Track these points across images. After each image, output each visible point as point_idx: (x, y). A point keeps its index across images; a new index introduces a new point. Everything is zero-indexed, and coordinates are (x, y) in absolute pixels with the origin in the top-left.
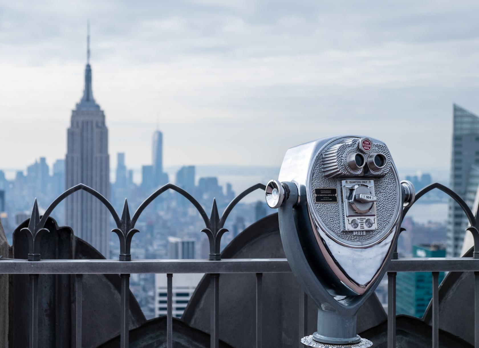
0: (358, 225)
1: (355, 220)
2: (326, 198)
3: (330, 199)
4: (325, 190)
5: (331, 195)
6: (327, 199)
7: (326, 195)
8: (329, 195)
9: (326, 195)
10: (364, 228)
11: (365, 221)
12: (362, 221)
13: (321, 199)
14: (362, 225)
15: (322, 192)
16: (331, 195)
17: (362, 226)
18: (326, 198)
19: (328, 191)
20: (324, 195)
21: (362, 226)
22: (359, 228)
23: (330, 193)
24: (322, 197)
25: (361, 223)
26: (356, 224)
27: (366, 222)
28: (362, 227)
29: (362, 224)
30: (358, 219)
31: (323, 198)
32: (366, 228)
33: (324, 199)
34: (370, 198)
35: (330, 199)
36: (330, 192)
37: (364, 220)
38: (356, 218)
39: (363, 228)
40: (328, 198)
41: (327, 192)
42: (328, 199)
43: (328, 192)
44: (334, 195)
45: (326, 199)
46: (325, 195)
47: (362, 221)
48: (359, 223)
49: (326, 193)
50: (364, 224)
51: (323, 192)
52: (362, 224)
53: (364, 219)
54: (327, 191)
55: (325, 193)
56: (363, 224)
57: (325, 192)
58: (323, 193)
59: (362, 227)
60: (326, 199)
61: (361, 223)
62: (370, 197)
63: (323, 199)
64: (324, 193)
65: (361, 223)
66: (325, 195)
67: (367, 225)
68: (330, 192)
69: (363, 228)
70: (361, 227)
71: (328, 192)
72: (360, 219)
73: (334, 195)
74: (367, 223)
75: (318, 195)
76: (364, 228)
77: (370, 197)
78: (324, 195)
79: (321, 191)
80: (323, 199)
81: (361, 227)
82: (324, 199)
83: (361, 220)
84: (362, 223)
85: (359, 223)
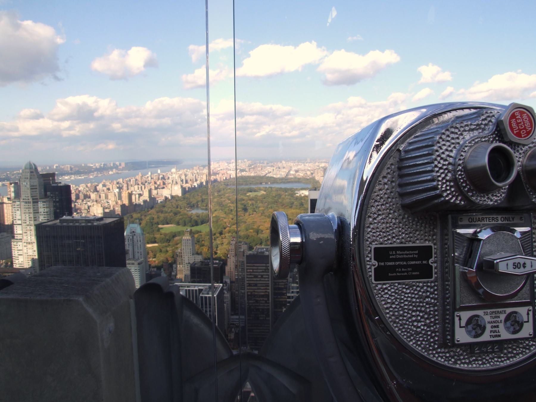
0: (483, 329)
1: (478, 316)
2: (403, 270)
6: (406, 274)
7: (405, 263)
8: (413, 263)
9: (405, 263)
10: (500, 336)
11: (503, 317)
13: (390, 275)
14: (494, 329)
17: (495, 331)
18: (403, 270)
19: (411, 252)
20: (397, 263)
21: (495, 331)
22: (486, 337)
23: (415, 256)
24: (393, 269)
25: (492, 324)
26: (480, 326)
27: (507, 319)
28: (495, 334)
29: (495, 327)
30: (486, 314)
31: (396, 272)
32: (505, 335)
33: (398, 274)
34: (524, 267)
38: (480, 312)
39: (496, 336)
40: (409, 269)
42: (407, 272)
43: (411, 254)
45: (404, 272)
46: (401, 263)
47: (496, 317)
48: (489, 322)
49: (405, 256)
50: (502, 326)
51: (396, 254)
52: (495, 327)
53: (501, 312)
54: (408, 253)
55: (402, 256)
56: (498, 327)
57: (403, 254)
58: (394, 257)
59: (495, 334)
60: (404, 272)
61: (494, 322)
62: (524, 264)
63: (395, 274)
64: (398, 256)
65: (494, 322)
66: (401, 263)
67: (507, 329)
69: (496, 336)
70: (492, 334)
71: (411, 254)
72: (493, 312)
74: (508, 324)
75: (382, 264)
76: (500, 336)
77: (524, 264)
78: (397, 263)
79: (391, 253)
80: (395, 274)
81: (492, 334)
82: (398, 274)
85: (489, 322)
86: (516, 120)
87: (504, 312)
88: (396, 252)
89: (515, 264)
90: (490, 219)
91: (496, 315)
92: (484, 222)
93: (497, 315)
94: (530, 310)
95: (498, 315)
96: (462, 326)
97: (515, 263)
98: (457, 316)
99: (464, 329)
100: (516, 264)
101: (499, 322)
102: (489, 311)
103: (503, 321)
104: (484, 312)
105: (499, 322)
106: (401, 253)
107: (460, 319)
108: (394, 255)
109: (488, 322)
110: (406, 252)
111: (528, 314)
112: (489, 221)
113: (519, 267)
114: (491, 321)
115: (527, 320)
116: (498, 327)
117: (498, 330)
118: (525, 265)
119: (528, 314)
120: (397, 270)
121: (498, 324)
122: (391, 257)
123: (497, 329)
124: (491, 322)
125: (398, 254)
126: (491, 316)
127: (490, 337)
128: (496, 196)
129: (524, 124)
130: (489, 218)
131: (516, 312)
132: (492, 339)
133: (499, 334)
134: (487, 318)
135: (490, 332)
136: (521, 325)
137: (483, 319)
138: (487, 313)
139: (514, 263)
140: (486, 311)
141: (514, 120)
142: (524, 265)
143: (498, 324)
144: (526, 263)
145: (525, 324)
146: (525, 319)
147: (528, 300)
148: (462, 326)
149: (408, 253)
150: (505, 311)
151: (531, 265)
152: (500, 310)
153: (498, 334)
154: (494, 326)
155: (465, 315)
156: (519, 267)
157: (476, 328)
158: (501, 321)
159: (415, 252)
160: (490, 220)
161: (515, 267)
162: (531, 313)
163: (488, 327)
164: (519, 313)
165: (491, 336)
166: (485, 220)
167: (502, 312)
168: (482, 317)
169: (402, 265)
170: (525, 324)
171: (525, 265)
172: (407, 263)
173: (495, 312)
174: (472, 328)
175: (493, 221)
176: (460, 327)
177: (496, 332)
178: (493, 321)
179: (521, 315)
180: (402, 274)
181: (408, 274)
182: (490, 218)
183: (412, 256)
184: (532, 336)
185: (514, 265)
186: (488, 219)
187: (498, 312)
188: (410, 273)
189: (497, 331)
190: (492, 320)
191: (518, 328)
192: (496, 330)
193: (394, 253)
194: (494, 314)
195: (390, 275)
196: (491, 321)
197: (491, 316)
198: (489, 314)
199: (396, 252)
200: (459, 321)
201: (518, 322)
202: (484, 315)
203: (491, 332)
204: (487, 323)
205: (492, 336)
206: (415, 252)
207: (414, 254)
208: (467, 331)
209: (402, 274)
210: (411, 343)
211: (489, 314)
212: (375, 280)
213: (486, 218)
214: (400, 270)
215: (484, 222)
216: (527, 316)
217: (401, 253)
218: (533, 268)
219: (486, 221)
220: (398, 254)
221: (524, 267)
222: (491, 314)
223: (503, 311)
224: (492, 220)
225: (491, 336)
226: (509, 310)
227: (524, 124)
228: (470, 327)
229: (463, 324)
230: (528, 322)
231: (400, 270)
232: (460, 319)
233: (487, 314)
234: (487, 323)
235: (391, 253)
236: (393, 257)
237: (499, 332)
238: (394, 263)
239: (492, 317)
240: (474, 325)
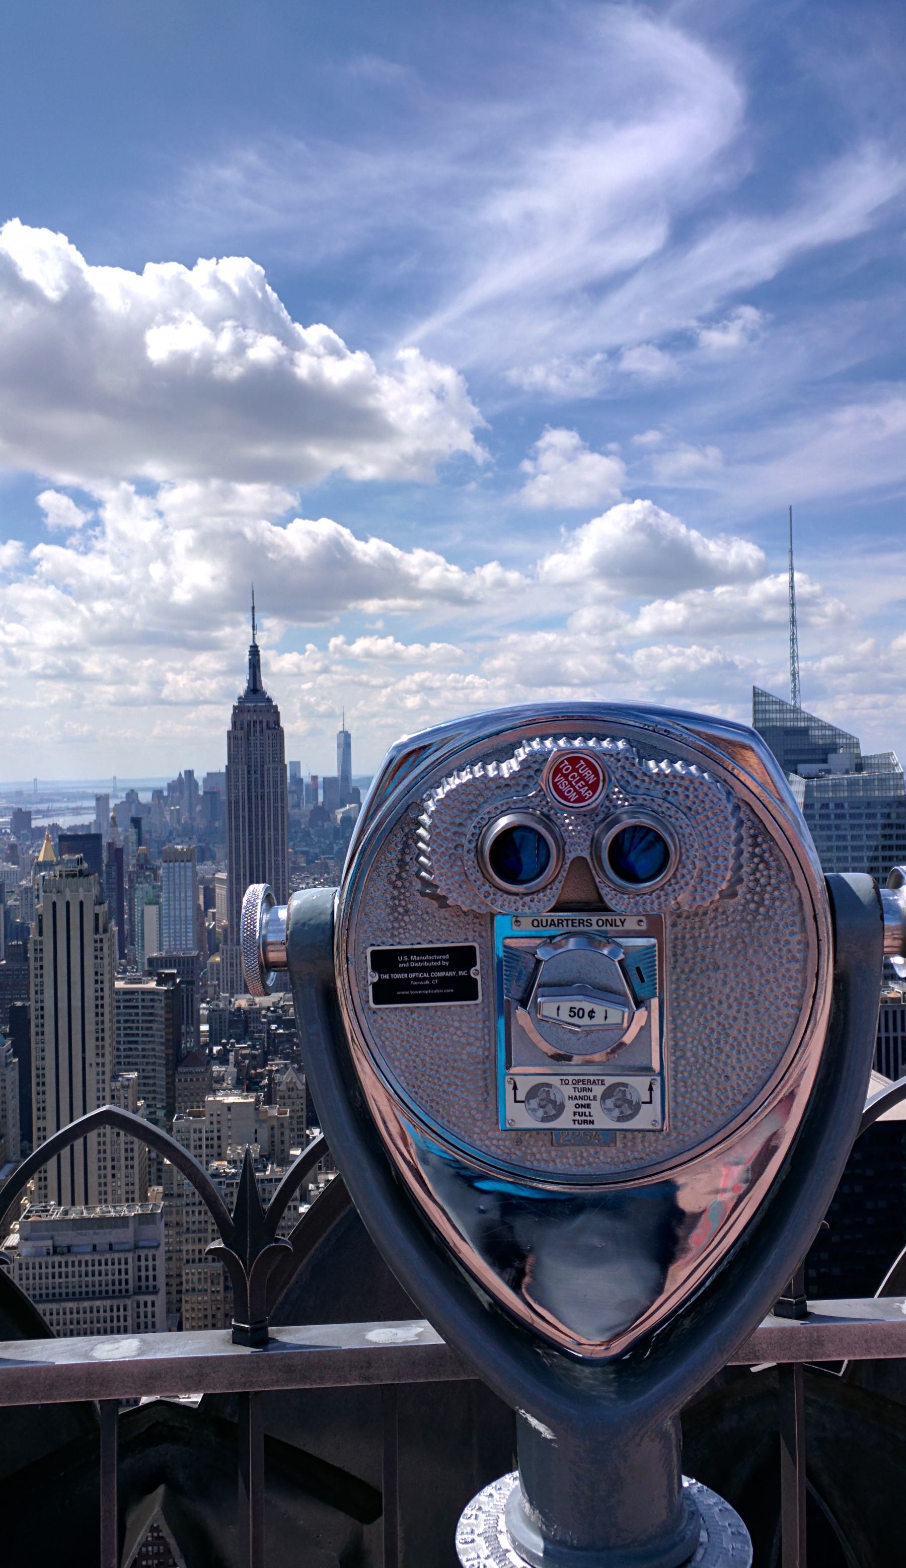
1: (549, 1085)
7: (426, 975)
8: (442, 974)
9: (426, 975)
10: (592, 1122)
11: (598, 1090)
12: (584, 1093)
13: (399, 993)
14: (580, 1110)
17: (584, 1114)
20: (413, 975)
21: (584, 1114)
22: (565, 1121)
23: (444, 963)
25: (576, 1102)
27: (605, 1096)
28: (583, 1118)
29: (583, 1106)
32: (603, 1120)
34: (591, 1017)
36: (445, 960)
37: (594, 1087)
39: (585, 1122)
41: (428, 961)
43: (437, 961)
46: (420, 975)
47: (584, 1090)
49: (426, 964)
50: (596, 1106)
51: (410, 961)
52: (583, 1106)
54: (430, 958)
55: (420, 964)
56: (588, 1106)
57: (422, 961)
58: (407, 965)
59: (583, 1118)
61: (582, 1098)
62: (592, 1011)
64: (413, 965)
65: (582, 1098)
66: (420, 975)
68: (445, 960)
69: (585, 1122)
70: (577, 1117)
71: (437, 961)
72: (578, 1081)
74: (610, 1103)
76: (592, 1122)
77: (592, 1011)
78: (413, 975)
79: (400, 959)
81: (577, 1117)
83: (580, 1086)
84: (580, 1102)
88: (409, 958)
93: (587, 1086)
95: (590, 1086)
96: (518, 1099)
100: (576, 1011)
101: (592, 1098)
103: (599, 1098)
105: (592, 1098)
106: (418, 958)
107: (515, 1088)
108: (405, 962)
111: (651, 1089)
113: (581, 1015)
119: (651, 1089)
121: (588, 1102)
122: (400, 965)
123: (587, 1110)
125: (414, 961)
131: (625, 1085)
132: (577, 1126)
133: (591, 1119)
136: (636, 1109)
142: (591, 1014)
143: (588, 1102)
145: (643, 1106)
148: (518, 1099)
149: (430, 958)
150: (602, 1081)
153: (588, 1118)
156: (581, 1015)
158: (595, 1098)
159: (444, 957)
161: (572, 1014)
163: (570, 1106)
164: (632, 1087)
165: (574, 1121)
168: (556, 1087)
176: (516, 1101)
179: (635, 1090)
187: (589, 1081)
190: (578, 1094)
193: (406, 958)
199: (409, 958)
200: (513, 1092)
203: (575, 1114)
206: (444, 957)
207: (441, 960)
220: (414, 961)
221: (591, 1017)
225: (574, 1121)
229: (521, 1096)
230: (650, 1102)
232: (515, 1088)
234: (567, 1098)
235: (400, 959)
236: (404, 965)
237: (590, 1115)
238: (406, 975)
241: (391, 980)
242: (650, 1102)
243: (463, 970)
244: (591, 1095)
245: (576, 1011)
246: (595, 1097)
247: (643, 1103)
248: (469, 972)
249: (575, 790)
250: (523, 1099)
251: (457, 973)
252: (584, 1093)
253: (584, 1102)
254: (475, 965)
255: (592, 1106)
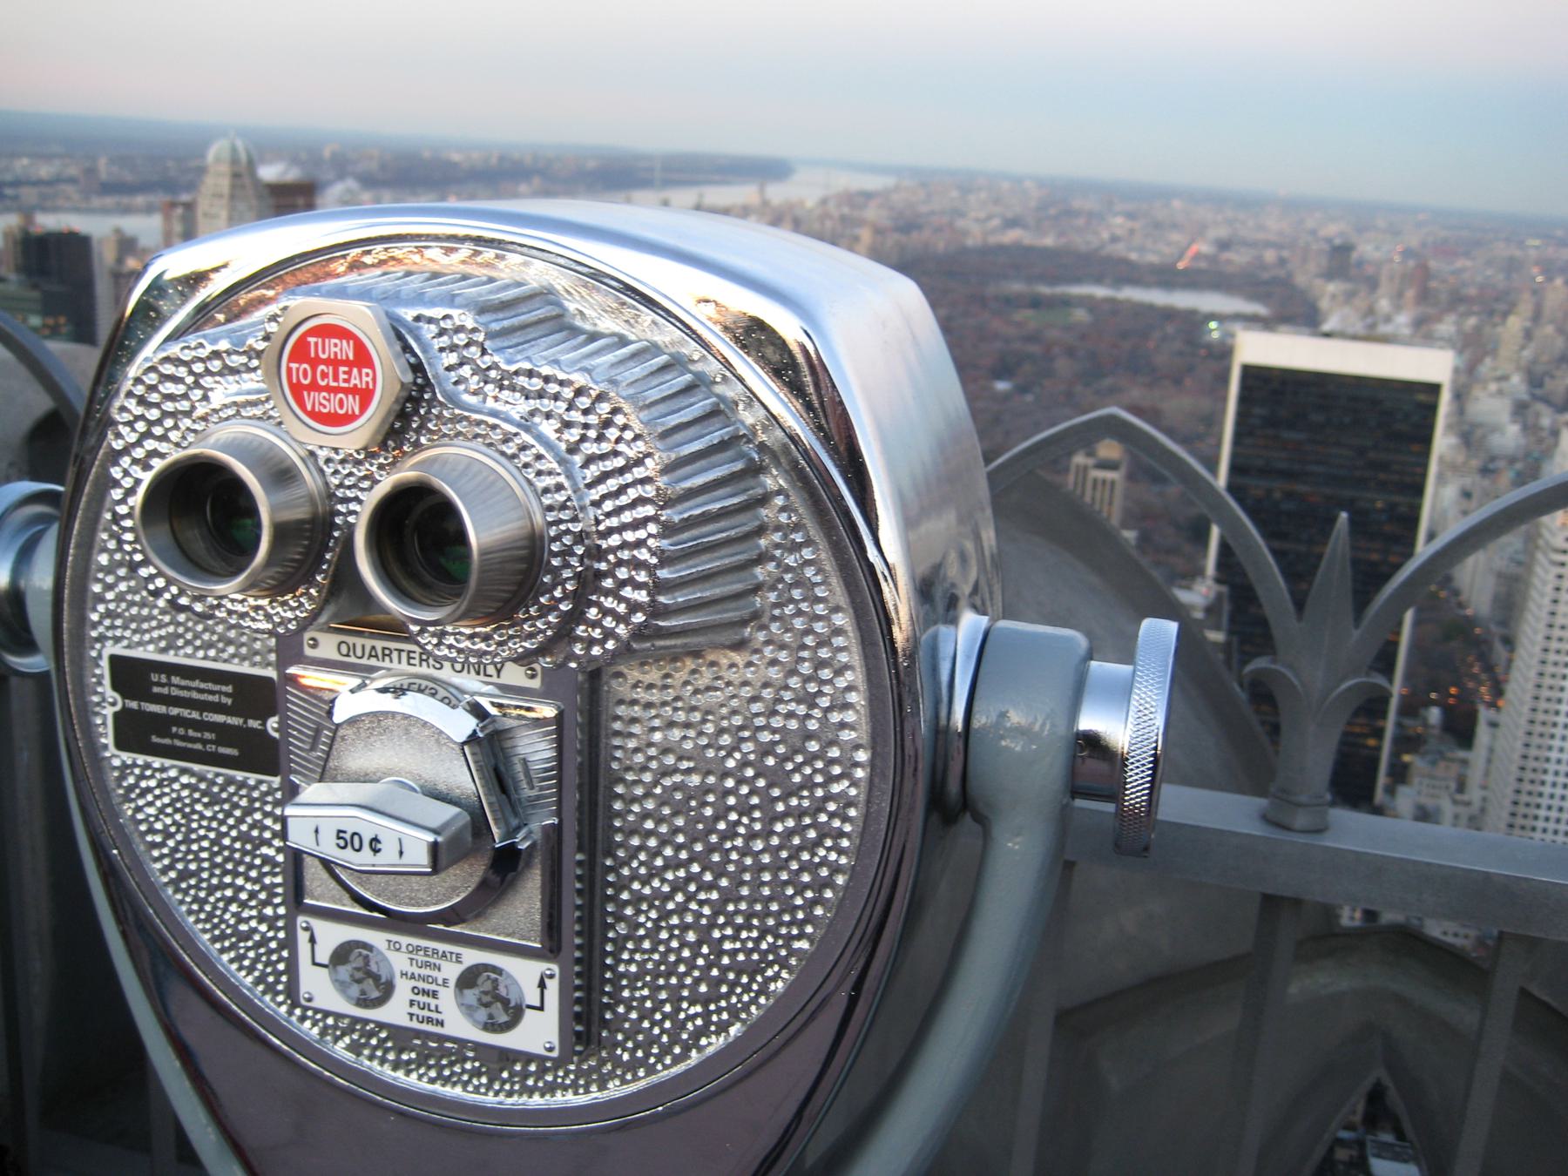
0: (387, 990)
2: (191, 733)
3: (223, 750)
4: (184, 677)
5: (235, 721)
6: (198, 746)
7: (195, 715)
8: (220, 718)
9: (195, 715)
10: (442, 1024)
11: (452, 971)
12: (425, 972)
14: (422, 999)
15: (159, 684)
16: (235, 721)
18: (191, 733)
19: (210, 686)
20: (175, 711)
22: (396, 1012)
23: (225, 700)
24: (163, 724)
25: (413, 983)
28: (426, 1013)
29: (425, 993)
32: (458, 1024)
33: (178, 743)
35: (223, 750)
36: (227, 695)
37: (444, 964)
39: (429, 1020)
40: (207, 735)
42: (205, 742)
44: (254, 724)
46: (185, 713)
47: (427, 965)
48: (403, 974)
49: (195, 695)
50: (447, 1001)
51: (170, 685)
52: (425, 993)
54: (203, 686)
56: (434, 994)
57: (189, 689)
58: (165, 691)
59: (426, 1013)
61: (424, 979)
62: (375, 840)
63: (167, 741)
64: (175, 692)
65: (424, 979)
66: (185, 713)
67: (468, 1010)
68: (227, 695)
69: (429, 1020)
70: (415, 1010)
72: (418, 949)
73: (254, 724)
74: (471, 995)
76: (442, 1024)
77: (375, 840)
78: (175, 711)
79: (154, 678)
80: (167, 741)
81: (415, 1010)
82: (178, 743)
84: (421, 985)
85: (403, 974)
86: (346, 362)
87: (454, 956)
88: (169, 678)
89: (341, 835)
90: (412, 655)
91: (427, 959)
92: (391, 661)
94: (551, 976)
95: (438, 962)
96: (318, 960)
97: (344, 832)
98: (306, 929)
99: (325, 971)
100: (348, 836)
101: (440, 982)
102: (405, 940)
103: (452, 983)
104: (389, 941)
105: (440, 982)
106: (184, 683)
107: (312, 940)
108: (163, 685)
109: (402, 974)
110: (196, 684)
111: (542, 985)
112: (409, 664)
113: (357, 845)
114: (413, 974)
115: (538, 1004)
116: (434, 994)
117: (437, 1007)
118: (379, 846)
119: (542, 985)
120: (174, 729)
123: (433, 1002)
124: (413, 977)
126: (412, 959)
127: (408, 1017)
128: (284, 604)
129: (328, 389)
130: (409, 652)
131: (498, 971)
132: (415, 1025)
133: (439, 1017)
134: (399, 962)
135: (408, 1003)
136: (515, 1014)
137: (385, 959)
138: (397, 946)
139: (340, 831)
140: (394, 937)
141: (351, 357)
143: (433, 987)
144: (379, 838)
145: (528, 1012)
146: (532, 997)
147: (535, 941)
149: (203, 686)
150: (458, 956)
151: (398, 848)
152: (442, 947)
153: (434, 1015)
154: (424, 990)
155: (331, 935)
156: (357, 845)
157: (364, 979)
159: (224, 688)
160: (412, 661)
161: (342, 843)
162: (553, 987)
163: (403, 989)
164: (509, 976)
165: (411, 1015)
166: (395, 655)
167: (448, 955)
169: (186, 719)
170: (528, 1012)
171: (379, 846)
172: (201, 715)
173: (426, 949)
174: (352, 976)
175: (424, 664)
176: (315, 964)
177: (429, 1010)
178: (419, 975)
179: (515, 983)
180: (190, 746)
181: (205, 747)
182: (414, 652)
183: (215, 698)
184: (555, 1054)
185: (339, 838)
186: (404, 655)
187: (435, 952)
188: (211, 748)
189: (433, 1008)
190: (417, 971)
191: (503, 1018)
192: (429, 1005)
194: (422, 953)
195: (155, 739)
196: (413, 974)
197: (412, 959)
198: (404, 949)
200: (309, 945)
201: (505, 1002)
202: (389, 948)
203: (412, 1003)
204: (398, 975)
205: (414, 1018)
207: (220, 693)
208: (336, 981)
209: (190, 746)
210: (225, 957)
211: (404, 949)
212: (121, 744)
213: (400, 651)
214: (182, 731)
215: (391, 661)
216: (539, 990)
217: (184, 683)
218: (405, 860)
219: (400, 662)
220: (177, 686)
222: (411, 952)
223: (451, 953)
224: (421, 660)
225: (411, 1015)
226: (472, 957)
227: (328, 389)
228: (344, 971)
229: (324, 955)
230: (541, 1008)
231: (182, 731)
232: (312, 940)
233: (398, 950)
237: (437, 1011)
239: (414, 962)
240: (358, 969)
241: (140, 712)
242: (541, 1008)
243: (255, 718)
244: (440, 976)
245: (348, 836)
246: (445, 981)
247: (530, 1007)
248: (264, 724)
249: (346, 391)
250: (325, 961)
251: (245, 722)
252: (425, 972)
253: (427, 986)
254: (116, 715)
255: (440, 995)
